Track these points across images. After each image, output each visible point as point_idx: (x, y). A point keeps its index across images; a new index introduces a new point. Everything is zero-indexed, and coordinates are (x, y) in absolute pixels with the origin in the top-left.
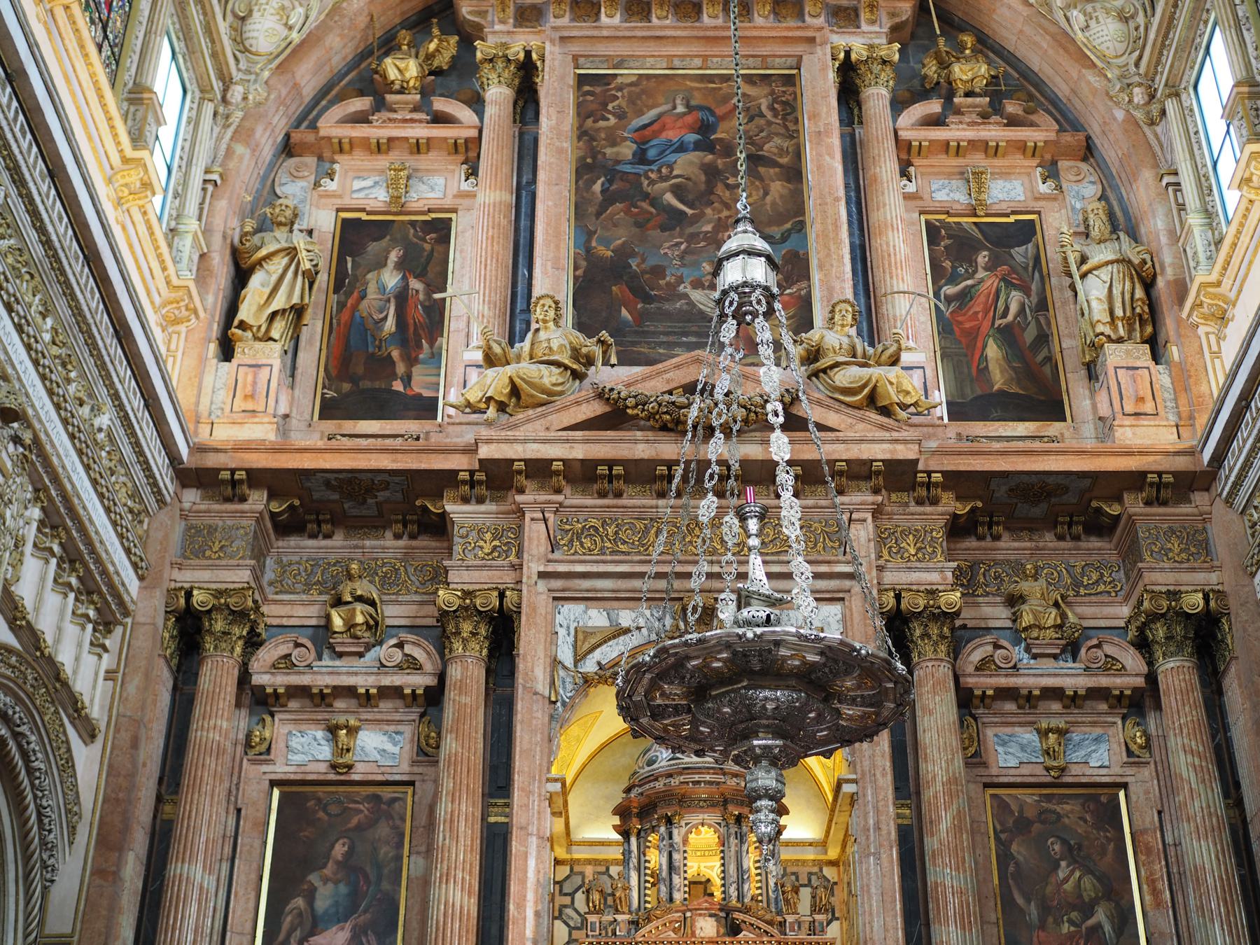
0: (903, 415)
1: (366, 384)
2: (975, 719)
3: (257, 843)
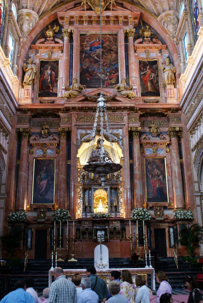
0: (132, 99)
1: (46, 91)
3: (32, 167)
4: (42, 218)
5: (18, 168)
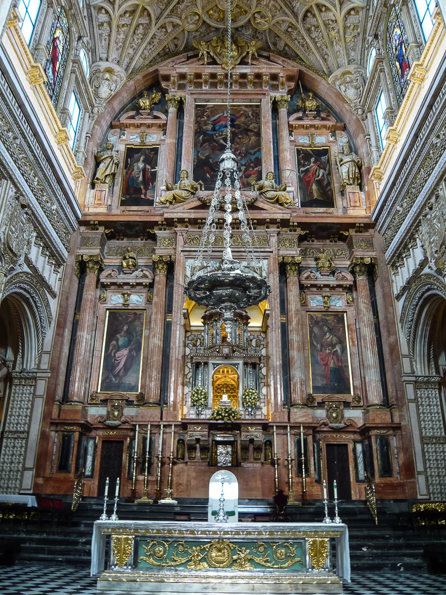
0: (286, 206)
1: (134, 196)
3: (102, 326)
4: (115, 419)
5: (75, 325)
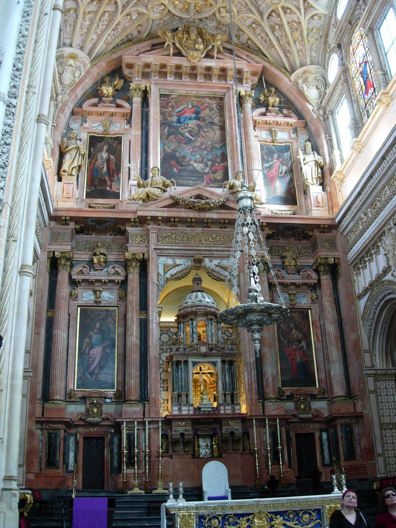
1: (99, 188)
2: (272, 290)
3: (75, 323)
4: (94, 415)
